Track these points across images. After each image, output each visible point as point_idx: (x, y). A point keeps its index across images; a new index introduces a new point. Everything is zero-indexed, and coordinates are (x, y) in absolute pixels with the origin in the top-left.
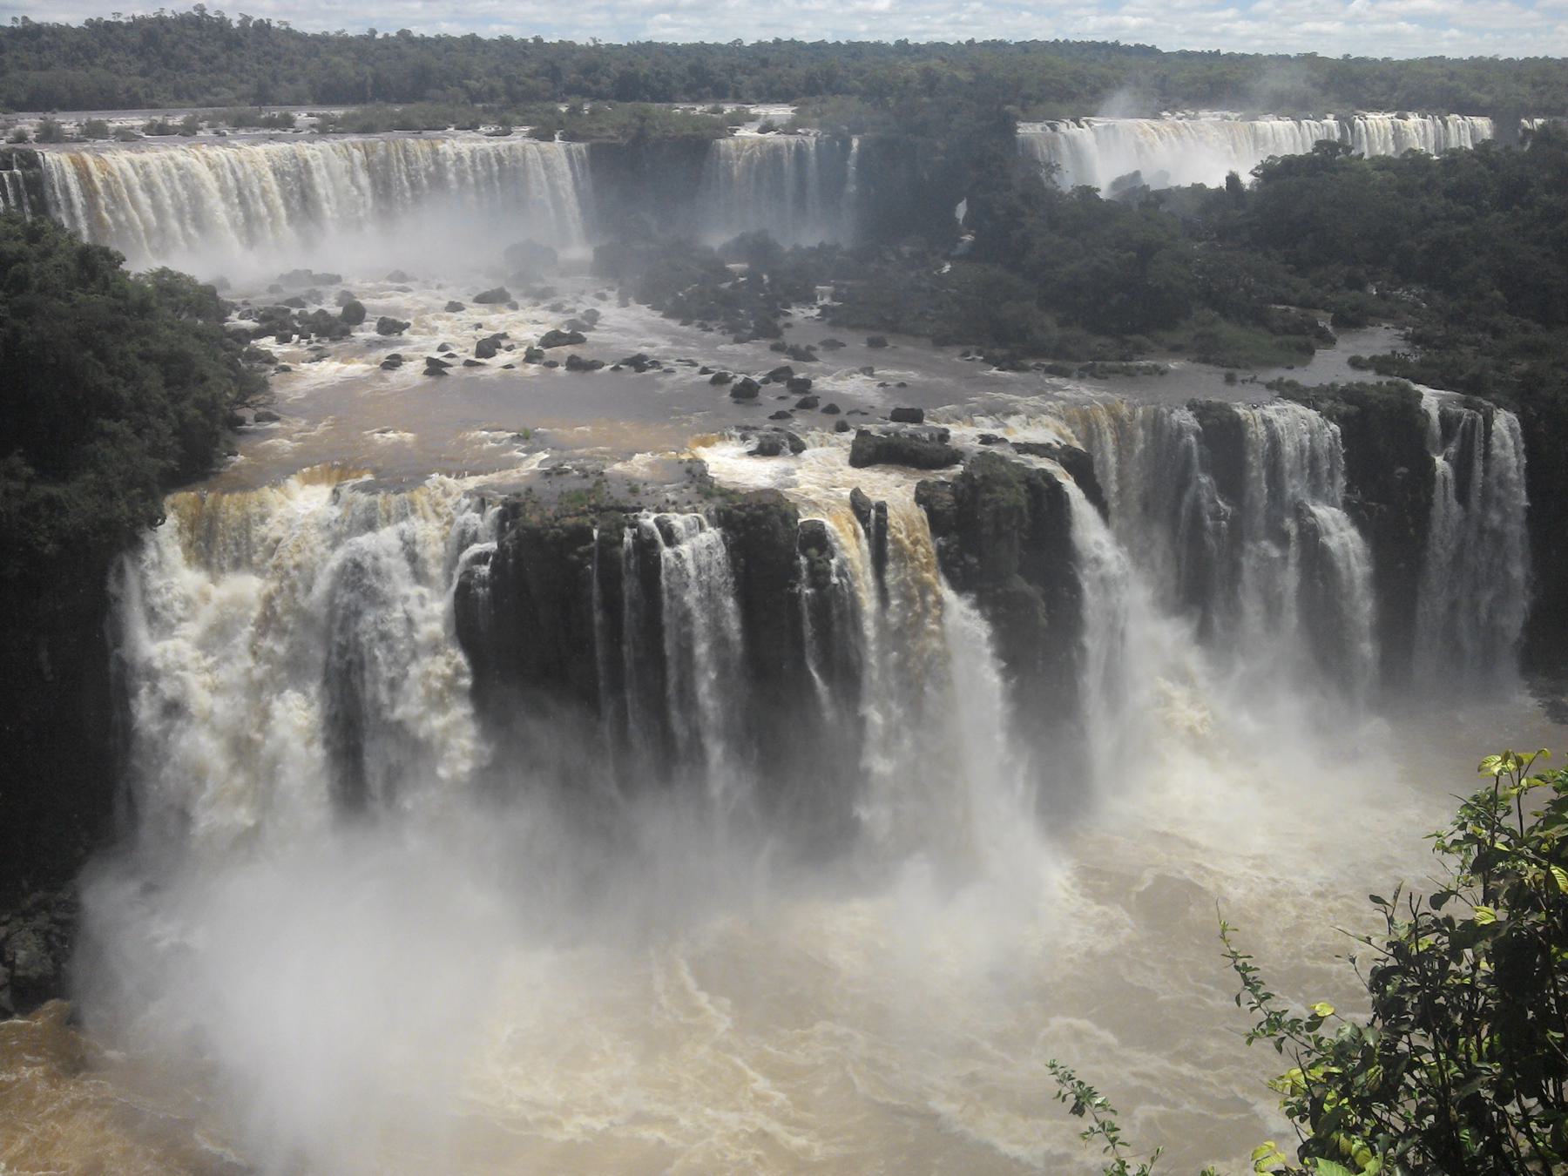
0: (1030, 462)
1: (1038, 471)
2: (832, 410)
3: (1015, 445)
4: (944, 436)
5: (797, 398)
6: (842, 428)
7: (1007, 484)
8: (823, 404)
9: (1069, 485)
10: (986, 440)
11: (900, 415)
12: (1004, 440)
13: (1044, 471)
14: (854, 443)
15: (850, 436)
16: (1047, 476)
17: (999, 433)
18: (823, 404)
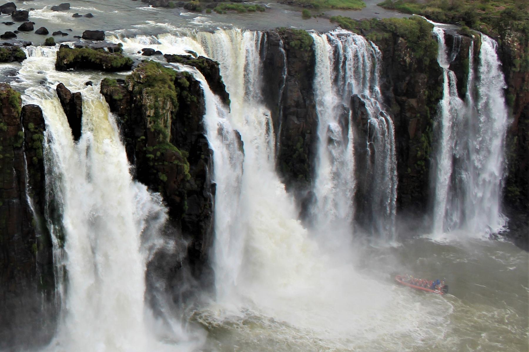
0: (177, 68)
1: (182, 73)
2: (44, 32)
3: (166, 56)
4: (118, 49)
5: (18, 25)
6: (49, 43)
7: (164, 81)
8: (36, 28)
9: (204, 85)
10: (148, 52)
11: (89, 35)
12: (159, 53)
13: (186, 73)
14: (58, 53)
15: (55, 49)
16: (189, 77)
17: (155, 48)
18: (36, 28)
